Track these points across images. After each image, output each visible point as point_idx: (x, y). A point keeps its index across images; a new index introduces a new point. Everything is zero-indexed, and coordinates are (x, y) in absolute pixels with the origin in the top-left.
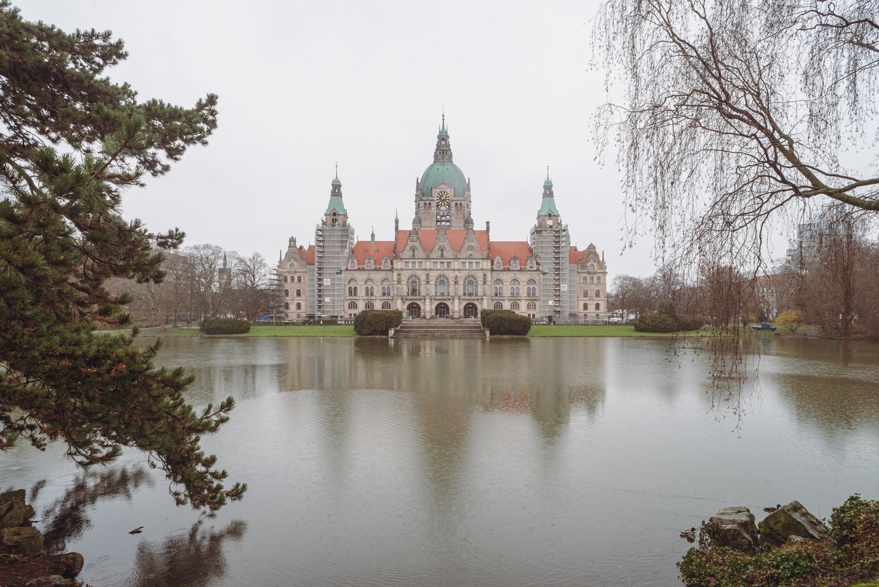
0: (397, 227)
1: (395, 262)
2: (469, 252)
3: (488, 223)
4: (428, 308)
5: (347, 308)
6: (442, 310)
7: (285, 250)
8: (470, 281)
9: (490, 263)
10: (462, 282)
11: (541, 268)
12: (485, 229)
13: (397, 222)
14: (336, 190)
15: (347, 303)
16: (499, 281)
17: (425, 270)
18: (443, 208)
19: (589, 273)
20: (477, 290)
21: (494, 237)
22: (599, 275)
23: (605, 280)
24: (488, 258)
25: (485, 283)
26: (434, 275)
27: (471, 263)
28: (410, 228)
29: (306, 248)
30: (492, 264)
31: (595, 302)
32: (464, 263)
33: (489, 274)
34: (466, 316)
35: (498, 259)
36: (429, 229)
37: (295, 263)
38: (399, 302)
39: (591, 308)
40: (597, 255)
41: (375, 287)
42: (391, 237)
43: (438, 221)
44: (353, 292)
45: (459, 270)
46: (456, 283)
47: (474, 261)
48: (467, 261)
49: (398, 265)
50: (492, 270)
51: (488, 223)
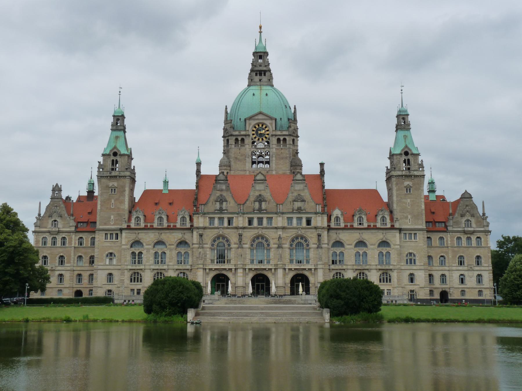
0: (198, 171)
1: (195, 218)
2: (297, 205)
3: (322, 165)
4: (240, 281)
5: (127, 281)
6: (261, 283)
7: (46, 202)
8: (299, 242)
10: (287, 246)
11: (397, 225)
12: (318, 172)
13: (199, 164)
14: (119, 123)
15: (127, 275)
16: (339, 244)
17: (236, 228)
18: (260, 145)
19: (465, 232)
20: (308, 256)
21: (330, 184)
22: (479, 235)
23: (487, 242)
24: (323, 213)
25: (319, 247)
26: (249, 235)
27: (300, 219)
28: (216, 171)
29: (74, 199)
30: (329, 220)
31: (476, 273)
32: (290, 219)
34: (294, 292)
35: (337, 212)
36: (242, 173)
38: (200, 273)
39: (471, 281)
40: (475, 207)
41: (168, 252)
42: (190, 183)
44: (137, 257)
45: (283, 228)
46: (280, 247)
47: (304, 216)
48: (295, 216)
49: (200, 221)
50: (329, 228)
51: (322, 165)
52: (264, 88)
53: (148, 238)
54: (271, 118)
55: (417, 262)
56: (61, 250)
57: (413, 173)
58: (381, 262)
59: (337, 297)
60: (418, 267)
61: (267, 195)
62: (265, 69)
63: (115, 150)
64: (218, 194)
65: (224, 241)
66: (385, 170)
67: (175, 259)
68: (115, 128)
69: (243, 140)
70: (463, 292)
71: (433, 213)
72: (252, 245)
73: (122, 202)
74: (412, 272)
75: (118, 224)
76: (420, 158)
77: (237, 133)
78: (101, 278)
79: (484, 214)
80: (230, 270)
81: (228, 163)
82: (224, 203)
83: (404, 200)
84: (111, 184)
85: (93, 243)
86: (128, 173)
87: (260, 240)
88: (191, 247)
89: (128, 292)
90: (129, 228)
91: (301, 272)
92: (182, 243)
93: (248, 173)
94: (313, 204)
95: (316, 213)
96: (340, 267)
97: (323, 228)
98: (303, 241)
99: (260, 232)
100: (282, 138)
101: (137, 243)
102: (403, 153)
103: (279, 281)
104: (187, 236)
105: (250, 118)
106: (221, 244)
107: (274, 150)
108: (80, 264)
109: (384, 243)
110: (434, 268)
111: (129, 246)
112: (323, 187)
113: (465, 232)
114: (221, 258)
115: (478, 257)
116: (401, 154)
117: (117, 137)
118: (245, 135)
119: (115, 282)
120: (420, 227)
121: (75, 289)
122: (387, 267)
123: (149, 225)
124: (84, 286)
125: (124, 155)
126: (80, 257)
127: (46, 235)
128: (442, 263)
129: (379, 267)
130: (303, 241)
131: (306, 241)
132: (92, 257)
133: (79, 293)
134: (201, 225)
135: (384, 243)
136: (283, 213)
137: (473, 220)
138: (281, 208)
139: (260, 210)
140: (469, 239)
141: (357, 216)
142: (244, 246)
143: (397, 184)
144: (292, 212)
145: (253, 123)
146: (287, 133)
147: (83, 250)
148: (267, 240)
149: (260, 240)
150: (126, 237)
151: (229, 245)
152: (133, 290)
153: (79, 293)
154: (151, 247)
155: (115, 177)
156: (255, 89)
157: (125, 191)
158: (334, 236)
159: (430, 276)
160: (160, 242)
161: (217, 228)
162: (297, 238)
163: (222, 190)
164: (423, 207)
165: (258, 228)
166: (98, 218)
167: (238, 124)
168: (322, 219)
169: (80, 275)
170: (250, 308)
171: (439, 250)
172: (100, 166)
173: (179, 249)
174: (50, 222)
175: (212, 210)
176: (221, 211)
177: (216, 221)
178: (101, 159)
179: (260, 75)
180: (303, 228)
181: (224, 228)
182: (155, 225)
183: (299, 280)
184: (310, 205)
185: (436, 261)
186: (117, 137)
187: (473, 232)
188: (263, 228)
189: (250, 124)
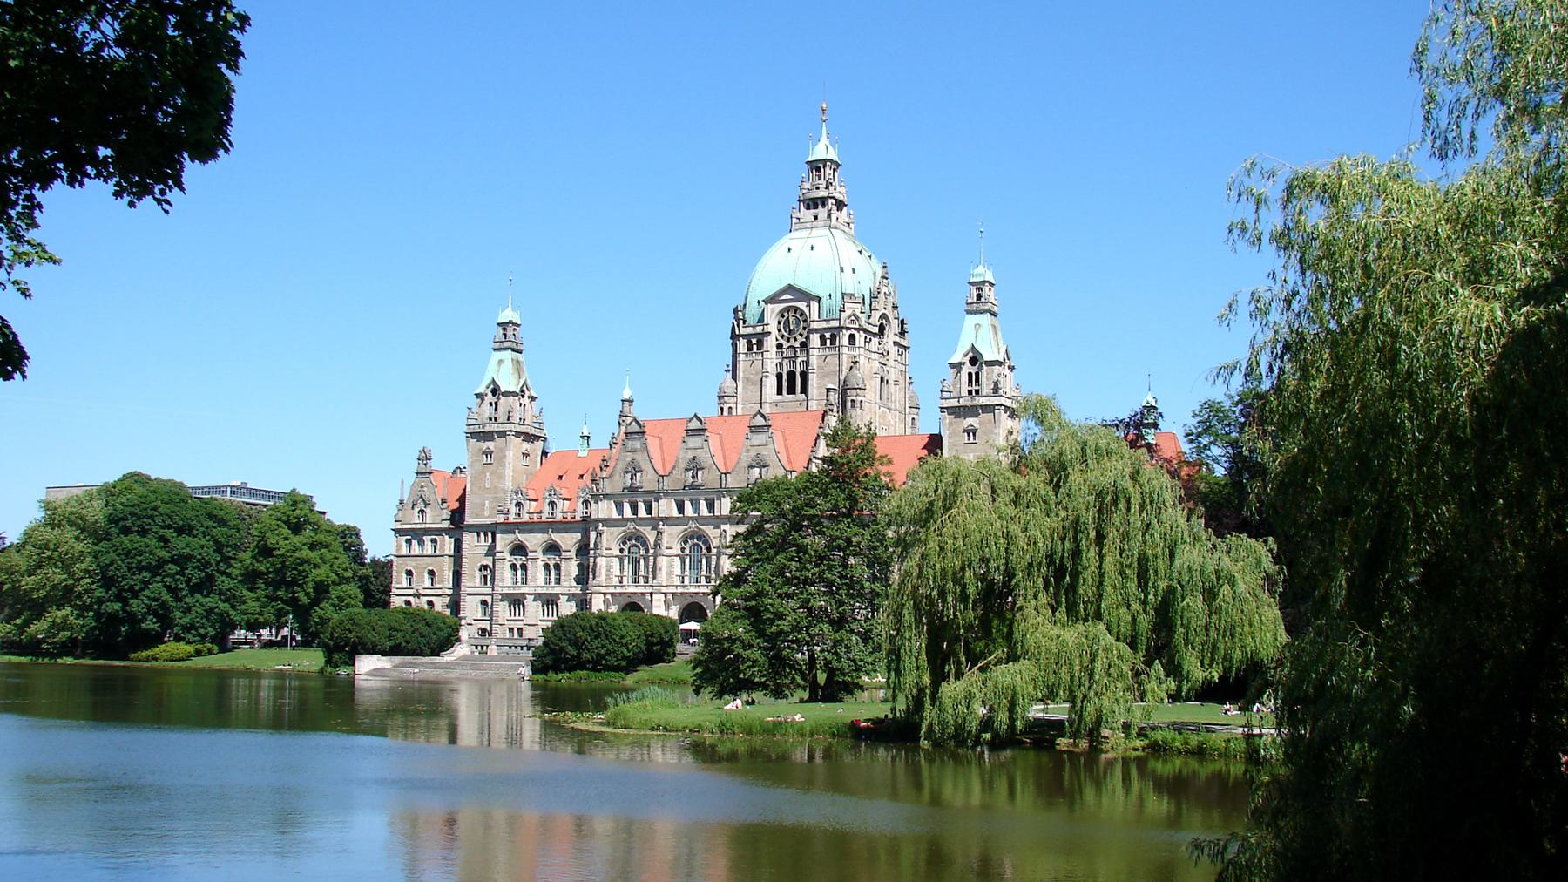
52: (815, 232)
54: (808, 297)
61: (703, 456)
62: (822, 193)
69: (760, 344)
73: (502, 477)
77: (750, 330)
80: (643, 594)
100: (828, 335)
102: (967, 360)
105: (772, 300)
117: (501, 361)
143: (951, 424)
151: (647, 551)
176: (632, 489)
186: (501, 361)
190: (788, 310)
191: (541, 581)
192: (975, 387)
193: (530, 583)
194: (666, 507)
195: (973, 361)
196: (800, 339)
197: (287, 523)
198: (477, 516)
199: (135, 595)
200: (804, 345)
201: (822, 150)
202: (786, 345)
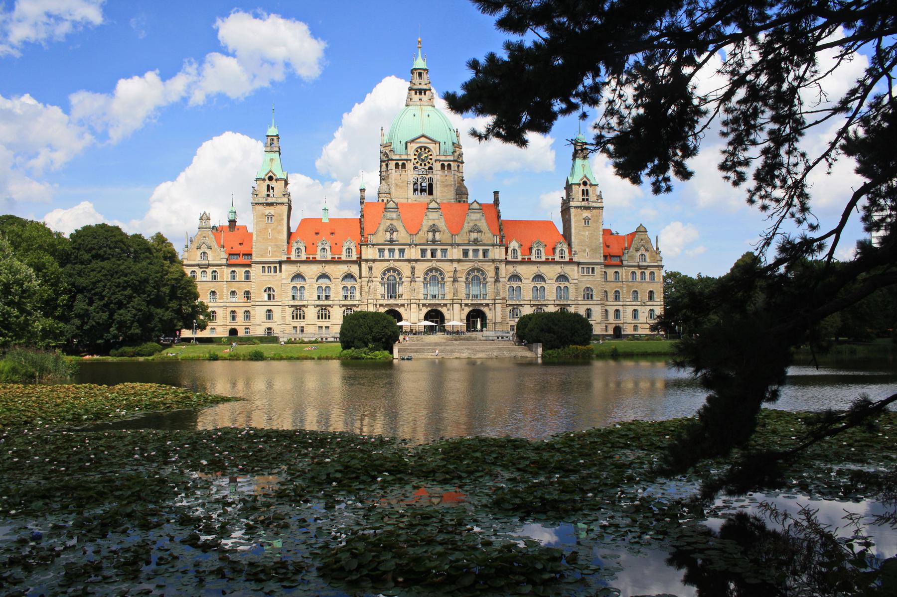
2: (474, 235)
3: (496, 193)
9: (503, 249)
12: (491, 201)
16: (516, 277)
19: (639, 267)
22: (652, 269)
25: (497, 281)
27: (476, 251)
31: (649, 308)
33: (502, 267)
35: (514, 245)
36: (405, 201)
37: (208, 251)
40: (648, 241)
41: (332, 287)
43: (415, 190)
45: (459, 261)
47: (481, 248)
49: (369, 253)
51: (496, 193)
53: (311, 271)
54: (434, 142)
55: (594, 297)
56: (211, 285)
57: (592, 204)
58: (559, 298)
59: (550, 331)
60: (595, 303)
61: (441, 224)
63: (271, 174)
64: (388, 223)
65: (395, 275)
66: (560, 201)
67: (342, 293)
68: (269, 149)
69: (404, 165)
70: (636, 328)
71: (608, 246)
72: (425, 279)
73: (280, 232)
74: (588, 307)
75: (277, 256)
76: (598, 189)
77: (397, 157)
78: (259, 314)
79: (657, 249)
80: (403, 305)
81: (387, 191)
82: (395, 233)
83: (582, 233)
84: (267, 212)
85: (248, 277)
86: (286, 200)
87: (434, 273)
88: (359, 281)
89: (289, 330)
90: (289, 261)
91: (477, 307)
92: (349, 276)
93: (410, 201)
94: (490, 235)
95: (493, 245)
96: (517, 302)
97: (501, 261)
98: (479, 275)
99: (434, 264)
100: (446, 164)
101: (299, 276)
103: (455, 319)
104: (354, 269)
105: (412, 141)
106: (392, 278)
107: (438, 177)
108: (234, 300)
109: (562, 277)
110: (609, 303)
111: (289, 281)
112: (499, 217)
113: (639, 267)
114: (392, 292)
115: (651, 292)
116: (579, 185)
117: (272, 160)
118: (407, 160)
119: (275, 319)
120: (598, 261)
121: (229, 328)
122: (565, 302)
123: (311, 257)
124: (240, 324)
125: (281, 179)
126: (233, 293)
127: (196, 269)
128: (617, 298)
129: (557, 302)
130: (479, 275)
131: (483, 273)
132: (247, 292)
133: (233, 332)
134: (370, 257)
135: (562, 277)
136: (458, 245)
137: (647, 254)
138: (458, 240)
139: (434, 242)
140: (642, 273)
141: (535, 249)
142: (417, 280)
143: (575, 216)
144: (469, 244)
145: (415, 146)
146: (452, 158)
147: (236, 285)
148: (441, 274)
149: (434, 273)
150: (286, 271)
151: (401, 279)
152: (295, 327)
153: (233, 332)
154: (314, 281)
155: (271, 204)
156: (413, 109)
157: (283, 219)
158: (511, 268)
159: (606, 311)
160: (324, 276)
161: (388, 261)
162: (473, 270)
163: (392, 219)
164: (601, 240)
165: (431, 261)
166: (254, 249)
167: (399, 148)
168: (500, 251)
169: (233, 312)
170: (430, 344)
171: (613, 285)
172: (255, 194)
173: (344, 283)
174: (199, 252)
175: (381, 241)
176: (391, 242)
177: (386, 253)
178: (254, 184)
179: (420, 93)
180: (480, 261)
181: (395, 261)
182: (318, 258)
183: (476, 316)
184: (487, 236)
185: (611, 296)
186: (272, 160)
187: (646, 267)
188: (438, 261)
189: (412, 148)
190: (420, 148)
191: (316, 298)
192: (585, 198)
193: (306, 297)
194: (413, 253)
195: (585, 184)
196: (428, 165)
197: (165, 258)
198: (262, 256)
199: (120, 305)
200: (431, 168)
201: (420, 63)
202: (420, 167)
